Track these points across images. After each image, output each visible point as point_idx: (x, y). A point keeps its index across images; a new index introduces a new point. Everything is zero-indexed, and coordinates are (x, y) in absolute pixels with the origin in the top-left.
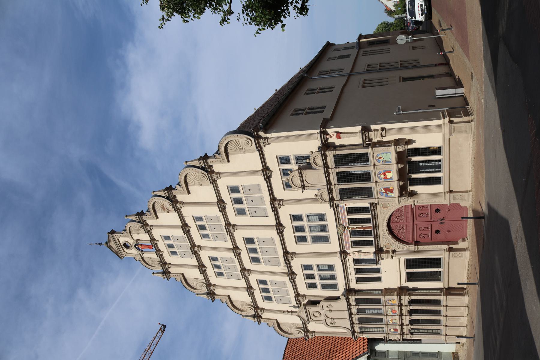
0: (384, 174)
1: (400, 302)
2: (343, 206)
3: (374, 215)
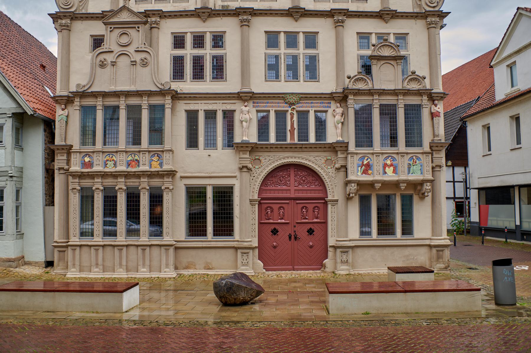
0: (392, 165)
2: (330, 107)
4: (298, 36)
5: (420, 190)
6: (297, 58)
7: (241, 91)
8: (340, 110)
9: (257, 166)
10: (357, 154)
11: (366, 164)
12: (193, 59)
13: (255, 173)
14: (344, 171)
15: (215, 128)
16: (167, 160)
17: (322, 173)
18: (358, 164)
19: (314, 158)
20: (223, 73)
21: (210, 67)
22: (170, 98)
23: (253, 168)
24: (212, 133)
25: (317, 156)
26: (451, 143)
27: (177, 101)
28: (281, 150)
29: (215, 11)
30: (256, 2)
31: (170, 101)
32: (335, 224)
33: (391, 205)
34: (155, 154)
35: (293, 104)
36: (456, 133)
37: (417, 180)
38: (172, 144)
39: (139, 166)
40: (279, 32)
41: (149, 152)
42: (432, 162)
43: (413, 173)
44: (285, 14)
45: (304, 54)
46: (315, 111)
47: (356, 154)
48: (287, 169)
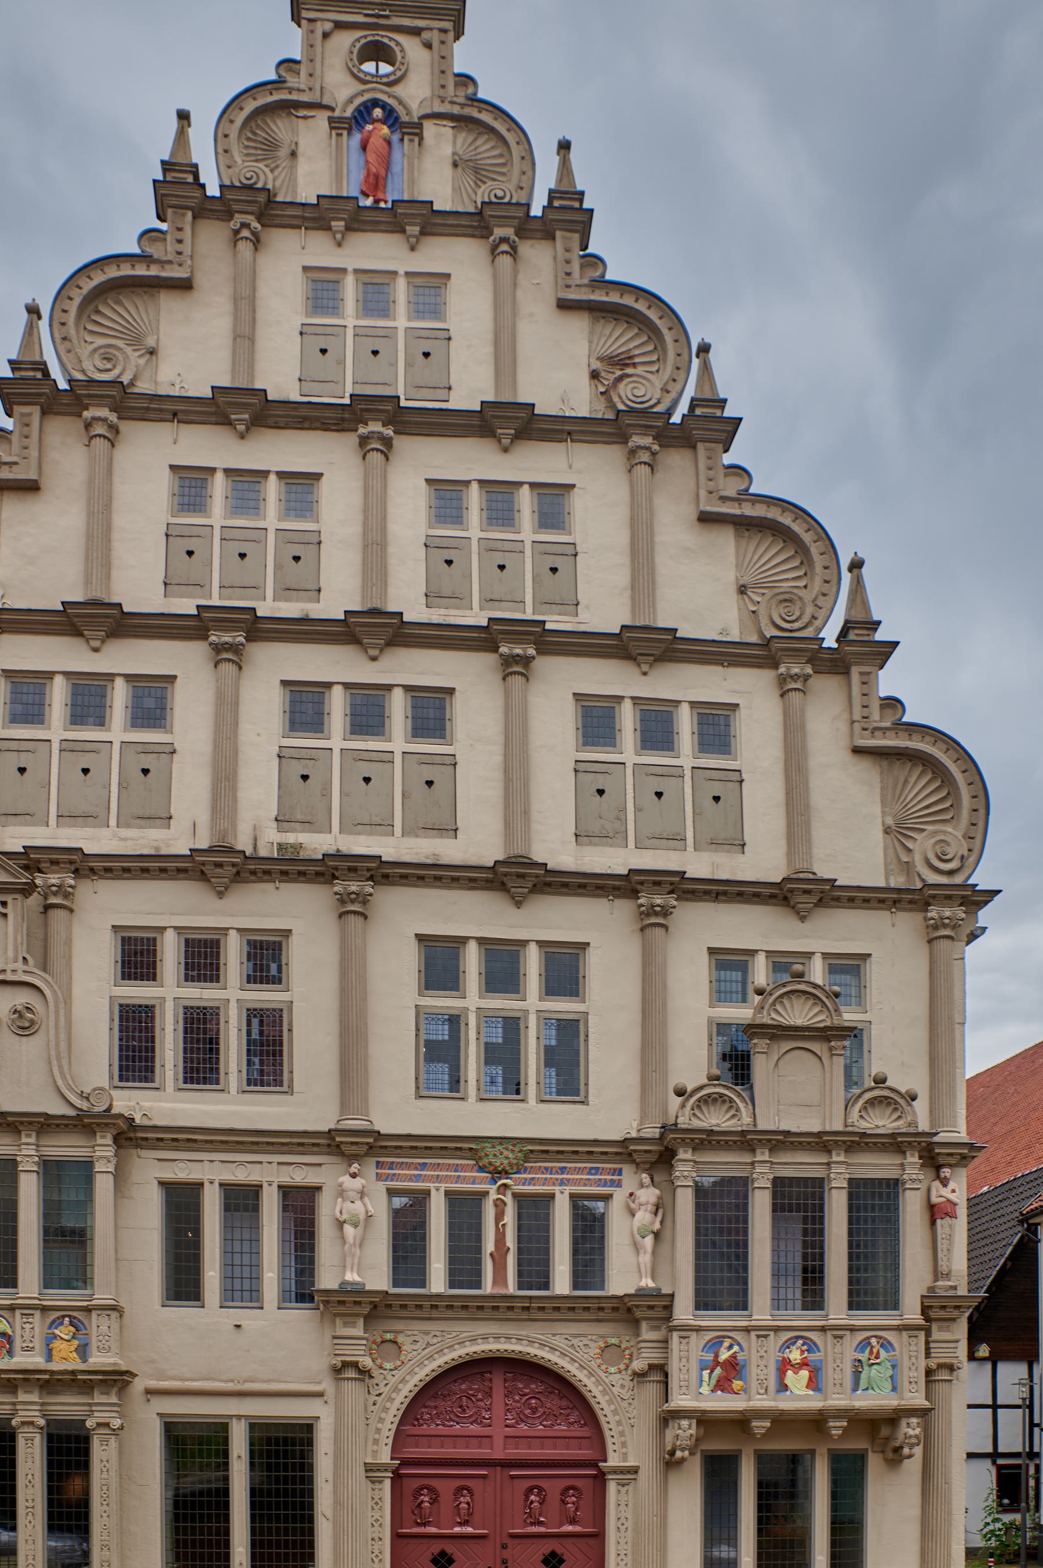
0: (804, 1364)
2: (619, 1184)
4: (521, 954)
5: (887, 1439)
6: (518, 1025)
7: (339, 1127)
8: (649, 1195)
9: (389, 1362)
10: (698, 1329)
11: (727, 1361)
12: (185, 1020)
13: (382, 1385)
14: (658, 1382)
15: (256, 1241)
16: (101, 1338)
17: (591, 1386)
18: (701, 1360)
19: (567, 1342)
20: (281, 1065)
21: (239, 1045)
22: (109, 1140)
23: (375, 1367)
24: (246, 1257)
25: (575, 1336)
26: (986, 1297)
27: (134, 1152)
28: (463, 1314)
29: (257, 861)
30: (391, 838)
31: (110, 1152)
32: (630, 1540)
33: (800, 1484)
34: (64, 1317)
35: (505, 1173)
36: (1007, 1259)
37: (881, 1410)
38: (117, 1287)
39: (10, 1353)
40: (463, 940)
41: (44, 1309)
42: (928, 1355)
43: (867, 1389)
44: (482, 879)
45: (541, 1014)
46: (572, 1196)
47: (697, 1330)
48: (482, 1374)
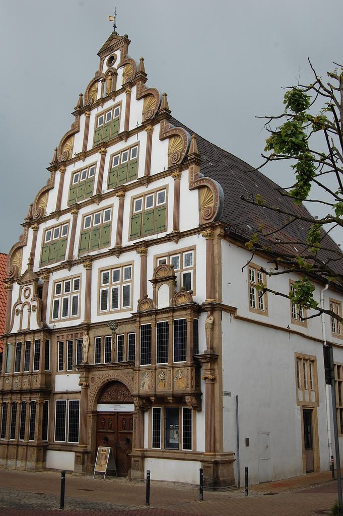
1: (35, 392)
3: (125, 365)
